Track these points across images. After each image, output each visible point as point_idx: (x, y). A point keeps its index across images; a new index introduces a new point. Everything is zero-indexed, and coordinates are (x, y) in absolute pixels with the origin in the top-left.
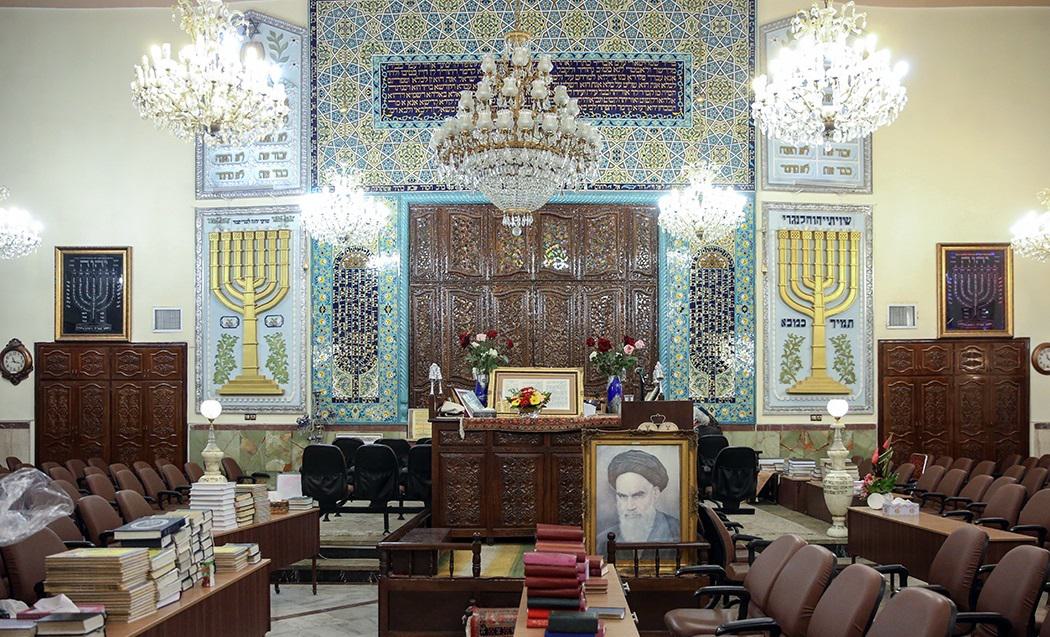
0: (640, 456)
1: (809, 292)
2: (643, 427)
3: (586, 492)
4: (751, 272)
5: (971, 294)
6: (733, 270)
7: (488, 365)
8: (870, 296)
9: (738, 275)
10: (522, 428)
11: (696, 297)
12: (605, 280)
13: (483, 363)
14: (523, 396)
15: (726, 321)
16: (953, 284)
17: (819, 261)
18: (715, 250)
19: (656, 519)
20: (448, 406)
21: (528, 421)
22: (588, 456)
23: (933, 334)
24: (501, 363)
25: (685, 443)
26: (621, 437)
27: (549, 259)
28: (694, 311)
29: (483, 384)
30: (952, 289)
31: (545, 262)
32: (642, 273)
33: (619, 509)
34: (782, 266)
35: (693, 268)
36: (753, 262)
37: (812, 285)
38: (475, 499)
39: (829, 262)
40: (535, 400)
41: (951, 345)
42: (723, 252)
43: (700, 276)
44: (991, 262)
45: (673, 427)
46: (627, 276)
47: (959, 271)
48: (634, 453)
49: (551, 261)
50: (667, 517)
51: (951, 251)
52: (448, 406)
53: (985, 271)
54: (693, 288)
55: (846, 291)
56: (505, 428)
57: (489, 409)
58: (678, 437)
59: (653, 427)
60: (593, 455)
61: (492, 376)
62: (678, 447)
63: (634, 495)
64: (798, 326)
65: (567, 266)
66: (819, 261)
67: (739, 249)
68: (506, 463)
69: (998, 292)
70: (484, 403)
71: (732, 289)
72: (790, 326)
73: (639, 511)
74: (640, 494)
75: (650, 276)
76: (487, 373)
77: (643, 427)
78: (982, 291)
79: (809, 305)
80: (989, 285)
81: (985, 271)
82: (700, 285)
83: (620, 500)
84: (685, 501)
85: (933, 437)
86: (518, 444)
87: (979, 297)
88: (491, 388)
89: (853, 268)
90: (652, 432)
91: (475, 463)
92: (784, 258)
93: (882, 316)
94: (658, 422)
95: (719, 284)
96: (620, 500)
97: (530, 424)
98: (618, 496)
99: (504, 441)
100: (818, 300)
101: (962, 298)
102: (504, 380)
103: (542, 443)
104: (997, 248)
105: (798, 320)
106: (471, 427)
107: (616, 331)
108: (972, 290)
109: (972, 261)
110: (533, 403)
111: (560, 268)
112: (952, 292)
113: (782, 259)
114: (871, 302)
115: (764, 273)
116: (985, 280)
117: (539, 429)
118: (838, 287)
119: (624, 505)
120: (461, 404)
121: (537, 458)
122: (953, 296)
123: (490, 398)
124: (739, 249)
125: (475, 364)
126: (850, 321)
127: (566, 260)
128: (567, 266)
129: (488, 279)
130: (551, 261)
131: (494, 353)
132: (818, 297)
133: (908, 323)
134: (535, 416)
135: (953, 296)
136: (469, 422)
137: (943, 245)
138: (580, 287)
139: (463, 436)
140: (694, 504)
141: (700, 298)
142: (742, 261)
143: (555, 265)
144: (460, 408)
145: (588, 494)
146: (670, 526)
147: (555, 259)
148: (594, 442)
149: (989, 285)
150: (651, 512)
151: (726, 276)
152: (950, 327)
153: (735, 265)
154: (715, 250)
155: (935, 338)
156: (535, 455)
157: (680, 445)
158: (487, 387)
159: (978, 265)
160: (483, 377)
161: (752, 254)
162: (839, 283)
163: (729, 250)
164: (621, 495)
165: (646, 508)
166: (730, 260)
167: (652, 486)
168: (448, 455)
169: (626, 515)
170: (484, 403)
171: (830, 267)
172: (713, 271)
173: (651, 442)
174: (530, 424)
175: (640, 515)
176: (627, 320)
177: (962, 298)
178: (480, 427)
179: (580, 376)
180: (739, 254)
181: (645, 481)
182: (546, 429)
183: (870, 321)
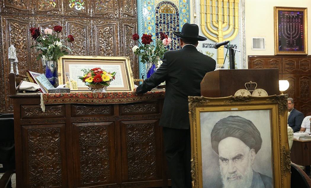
0: (239, 121)
1: (216, 29)
2: (239, 93)
3: (194, 160)
4: (188, 16)
5: (289, 33)
6: (178, 15)
7: (56, 53)
8: (244, 32)
9: (181, 17)
10: (96, 101)
11: (159, 29)
12: (106, 18)
13: (51, 53)
14: (94, 74)
15: (175, 44)
16: (281, 28)
17: (220, 13)
18: (168, 3)
19: (254, 179)
20: (25, 85)
21: (101, 96)
22: (194, 123)
23: (272, 54)
24: (65, 52)
25: (274, 108)
26: (222, 103)
27: (72, 3)
28: (158, 37)
29: (52, 69)
30: (281, 30)
31: (70, 5)
32: (128, 15)
33: (221, 174)
34: (202, 14)
35: (157, 13)
36: (189, 11)
37: (217, 25)
38: (57, 164)
39: (225, 14)
40: (106, 77)
41: (281, 58)
42: (173, 5)
43: (161, 17)
44: (298, 17)
45: (263, 93)
46: (119, 16)
47: (284, 21)
48: (231, 119)
49: (73, 4)
50: (262, 176)
51: (282, 11)
52: (25, 85)
53: (298, 21)
54: (157, 24)
55: (233, 29)
56: (81, 101)
57: (61, 86)
58: (270, 102)
59: (246, 93)
60: (197, 121)
61: (60, 62)
62: (269, 111)
63: (234, 159)
64: (211, 47)
65: (84, 8)
66: (220, 13)
67: (181, 3)
68: (84, 131)
69: (301, 32)
70: (54, 83)
71: (178, 26)
72: (207, 47)
73: (239, 173)
74: (238, 157)
75: (133, 17)
76: (54, 60)
77: (239, 93)
78: (294, 31)
79: (216, 36)
80: (297, 28)
81: (295, 21)
82: (160, 23)
83: (223, 165)
84: (277, 160)
85: (305, 104)
86: (93, 115)
87: (293, 35)
88: (60, 71)
89: (236, 17)
90: (250, 98)
91: (56, 133)
92: (204, 11)
93: (250, 43)
94: (251, 88)
95: (171, 22)
96: (223, 165)
97: (103, 98)
98: (220, 161)
99: (80, 112)
100: (220, 34)
101: (285, 34)
102: (70, 65)
103: (112, 113)
104: (300, 10)
105: (211, 44)
106: (51, 101)
107: (114, 48)
108: (290, 30)
109: (290, 16)
110: (104, 80)
111: (80, 9)
112: (281, 32)
113: (202, 11)
114: (244, 36)
115: (195, 17)
116: (295, 26)
117: (110, 101)
118: (229, 27)
119: (226, 169)
120: (35, 82)
121: (109, 126)
122: (281, 34)
123: (60, 79)
124: (181, 3)
125: (45, 52)
126: (235, 45)
127: (83, 4)
128: (84, 8)
129: (33, 13)
130: (73, 4)
131: (59, 44)
132: (220, 32)
133: (261, 47)
134: (104, 91)
135: (281, 34)
136: (49, 97)
137: (277, 7)
138: (92, 21)
139: (43, 108)
140: (287, 164)
141: (161, 30)
142: (183, 10)
143: (76, 7)
144: (37, 87)
145: (196, 161)
146: (265, 184)
147: (76, 4)
148: (198, 109)
149: (297, 28)
150: (249, 173)
151: (175, 18)
152: (281, 49)
153: (179, 12)
154: (168, 3)
155: (273, 54)
156: (107, 123)
157: (271, 109)
158: (56, 70)
159: (292, 19)
160: (52, 63)
161: (188, 7)
162: (229, 25)
163: (176, 4)
164: (224, 160)
165: (245, 170)
166: (177, 9)
167: (247, 149)
168: (30, 127)
169: (228, 178)
170: (54, 83)
171: (225, 16)
172: (168, 15)
173: (247, 107)
174: (103, 98)
175: (240, 177)
176: (120, 42)
177: (285, 34)
178: (59, 101)
179: (128, 63)
180: (181, 6)
181: (242, 144)
182: (116, 101)
183: (244, 46)
